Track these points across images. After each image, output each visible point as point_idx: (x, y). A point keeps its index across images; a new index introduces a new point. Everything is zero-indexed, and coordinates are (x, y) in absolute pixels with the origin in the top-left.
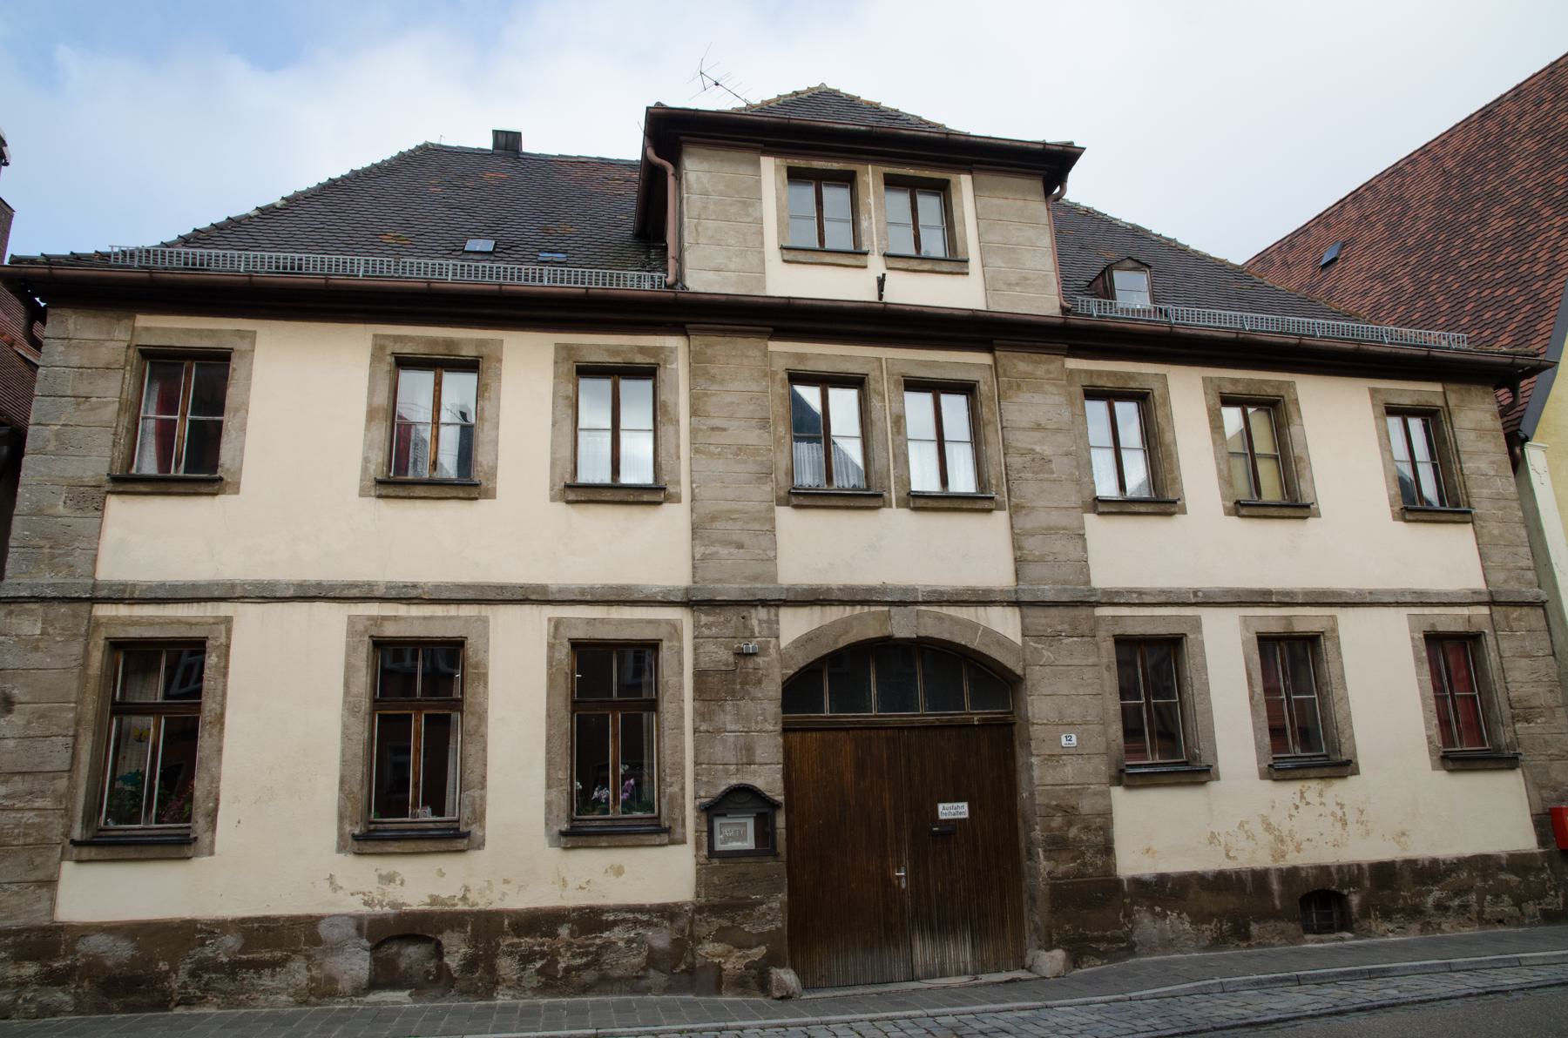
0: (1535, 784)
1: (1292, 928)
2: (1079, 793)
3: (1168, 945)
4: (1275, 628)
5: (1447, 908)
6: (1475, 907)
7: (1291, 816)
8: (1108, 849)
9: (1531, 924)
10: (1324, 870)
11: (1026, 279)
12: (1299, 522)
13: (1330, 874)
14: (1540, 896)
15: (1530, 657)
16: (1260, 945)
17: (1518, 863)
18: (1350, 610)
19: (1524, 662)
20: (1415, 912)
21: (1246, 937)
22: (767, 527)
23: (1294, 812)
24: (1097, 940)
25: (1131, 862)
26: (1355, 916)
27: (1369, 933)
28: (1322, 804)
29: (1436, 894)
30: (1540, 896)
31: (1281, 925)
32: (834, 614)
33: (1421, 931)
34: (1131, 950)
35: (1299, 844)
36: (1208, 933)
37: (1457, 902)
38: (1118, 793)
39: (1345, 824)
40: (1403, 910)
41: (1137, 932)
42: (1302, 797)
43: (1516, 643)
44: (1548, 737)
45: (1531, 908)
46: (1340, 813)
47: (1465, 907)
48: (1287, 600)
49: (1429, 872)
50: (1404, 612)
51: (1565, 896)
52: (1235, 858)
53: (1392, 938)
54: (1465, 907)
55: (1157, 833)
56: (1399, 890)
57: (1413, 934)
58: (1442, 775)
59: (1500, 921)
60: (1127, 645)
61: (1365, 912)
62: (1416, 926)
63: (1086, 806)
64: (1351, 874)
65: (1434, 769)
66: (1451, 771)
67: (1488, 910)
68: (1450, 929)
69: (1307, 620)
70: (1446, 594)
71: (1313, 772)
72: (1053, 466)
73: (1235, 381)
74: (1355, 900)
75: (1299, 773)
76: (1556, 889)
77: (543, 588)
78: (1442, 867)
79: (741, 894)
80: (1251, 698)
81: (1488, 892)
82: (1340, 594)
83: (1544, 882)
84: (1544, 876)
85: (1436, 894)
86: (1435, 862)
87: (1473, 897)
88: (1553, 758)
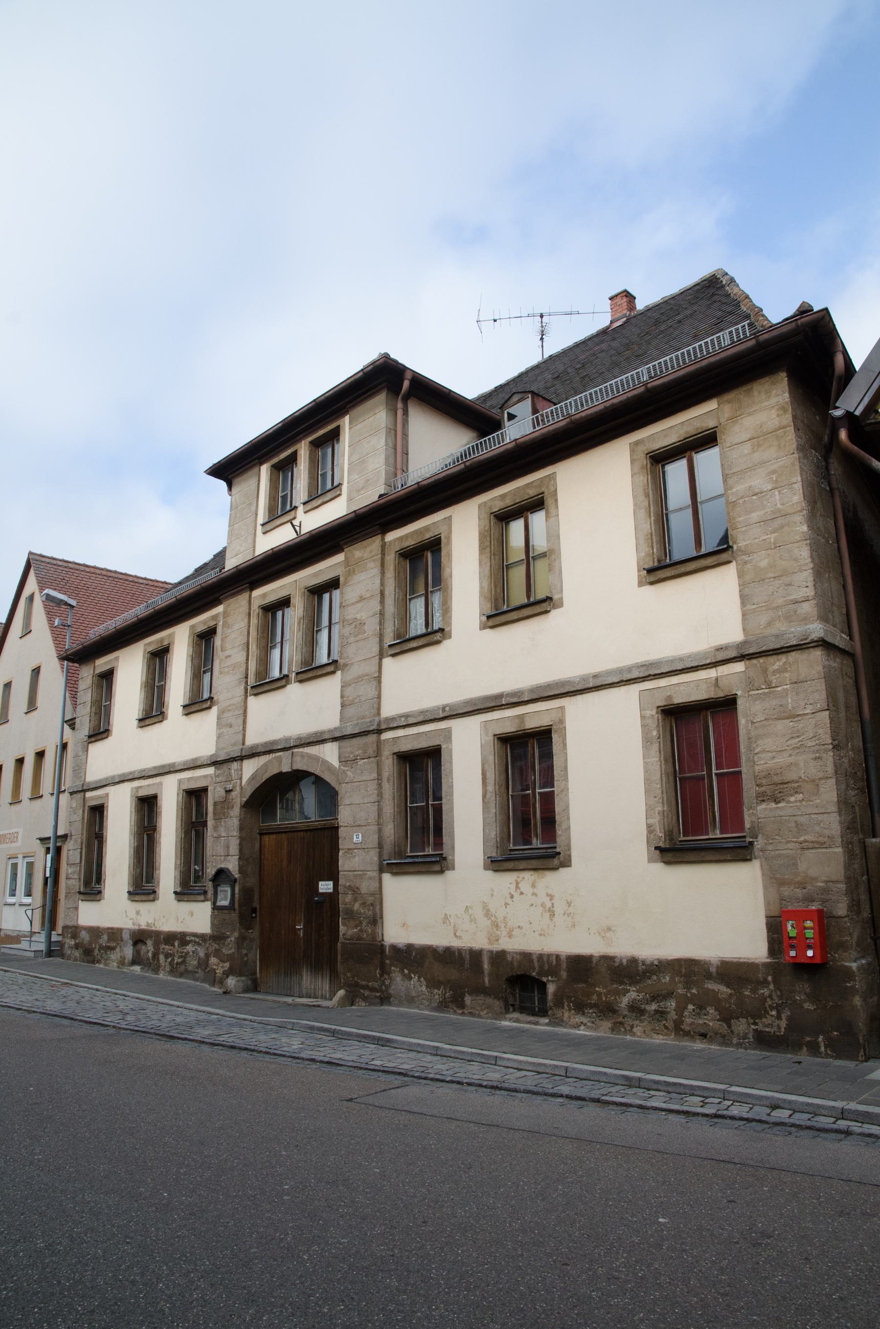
0: (774, 879)
1: (497, 1004)
2: (361, 877)
3: (411, 1001)
4: (509, 728)
5: (642, 1012)
6: (673, 1015)
7: (506, 904)
8: (376, 920)
9: (739, 1045)
10: (526, 956)
11: (368, 480)
12: (543, 617)
13: (532, 961)
14: (756, 1015)
15: (792, 717)
16: (471, 1014)
17: (733, 973)
18: (579, 698)
19: (781, 726)
20: (607, 1010)
21: (462, 1005)
22: (682, 545)
23: (509, 901)
24: (366, 987)
25: (397, 931)
26: (550, 1004)
27: (559, 1022)
28: (534, 894)
29: (633, 995)
30: (756, 1015)
31: (489, 1000)
32: (263, 759)
33: (613, 1030)
34: (385, 999)
35: (511, 930)
36: (437, 997)
37: (653, 1007)
38: (387, 877)
39: (552, 914)
40: (595, 1006)
41: (393, 987)
42: (517, 887)
43: (774, 702)
44: (803, 820)
45: (741, 1026)
46: (549, 905)
47: (661, 1014)
48: (515, 700)
49: (628, 972)
50: (635, 689)
51: (789, 1019)
52: (460, 937)
53: (582, 1032)
54: (661, 1014)
55: (415, 912)
56: (594, 985)
57: (603, 1030)
58: (659, 869)
59: (704, 1035)
60: (404, 758)
61: (559, 1004)
62: (607, 1024)
63: (366, 887)
64: (550, 963)
65: (651, 860)
66: (668, 863)
67: (688, 1021)
68: (642, 1034)
69: (536, 716)
70: (681, 659)
71: (523, 864)
72: (366, 627)
73: (503, 497)
74: (551, 988)
75: (510, 865)
76: (779, 1008)
77: (173, 765)
78: (641, 968)
79: (223, 931)
80: (484, 796)
81: (690, 1001)
82: (562, 683)
83: (763, 999)
84: (765, 992)
85: (633, 995)
86: (633, 961)
87: (672, 1004)
88: (804, 847)
